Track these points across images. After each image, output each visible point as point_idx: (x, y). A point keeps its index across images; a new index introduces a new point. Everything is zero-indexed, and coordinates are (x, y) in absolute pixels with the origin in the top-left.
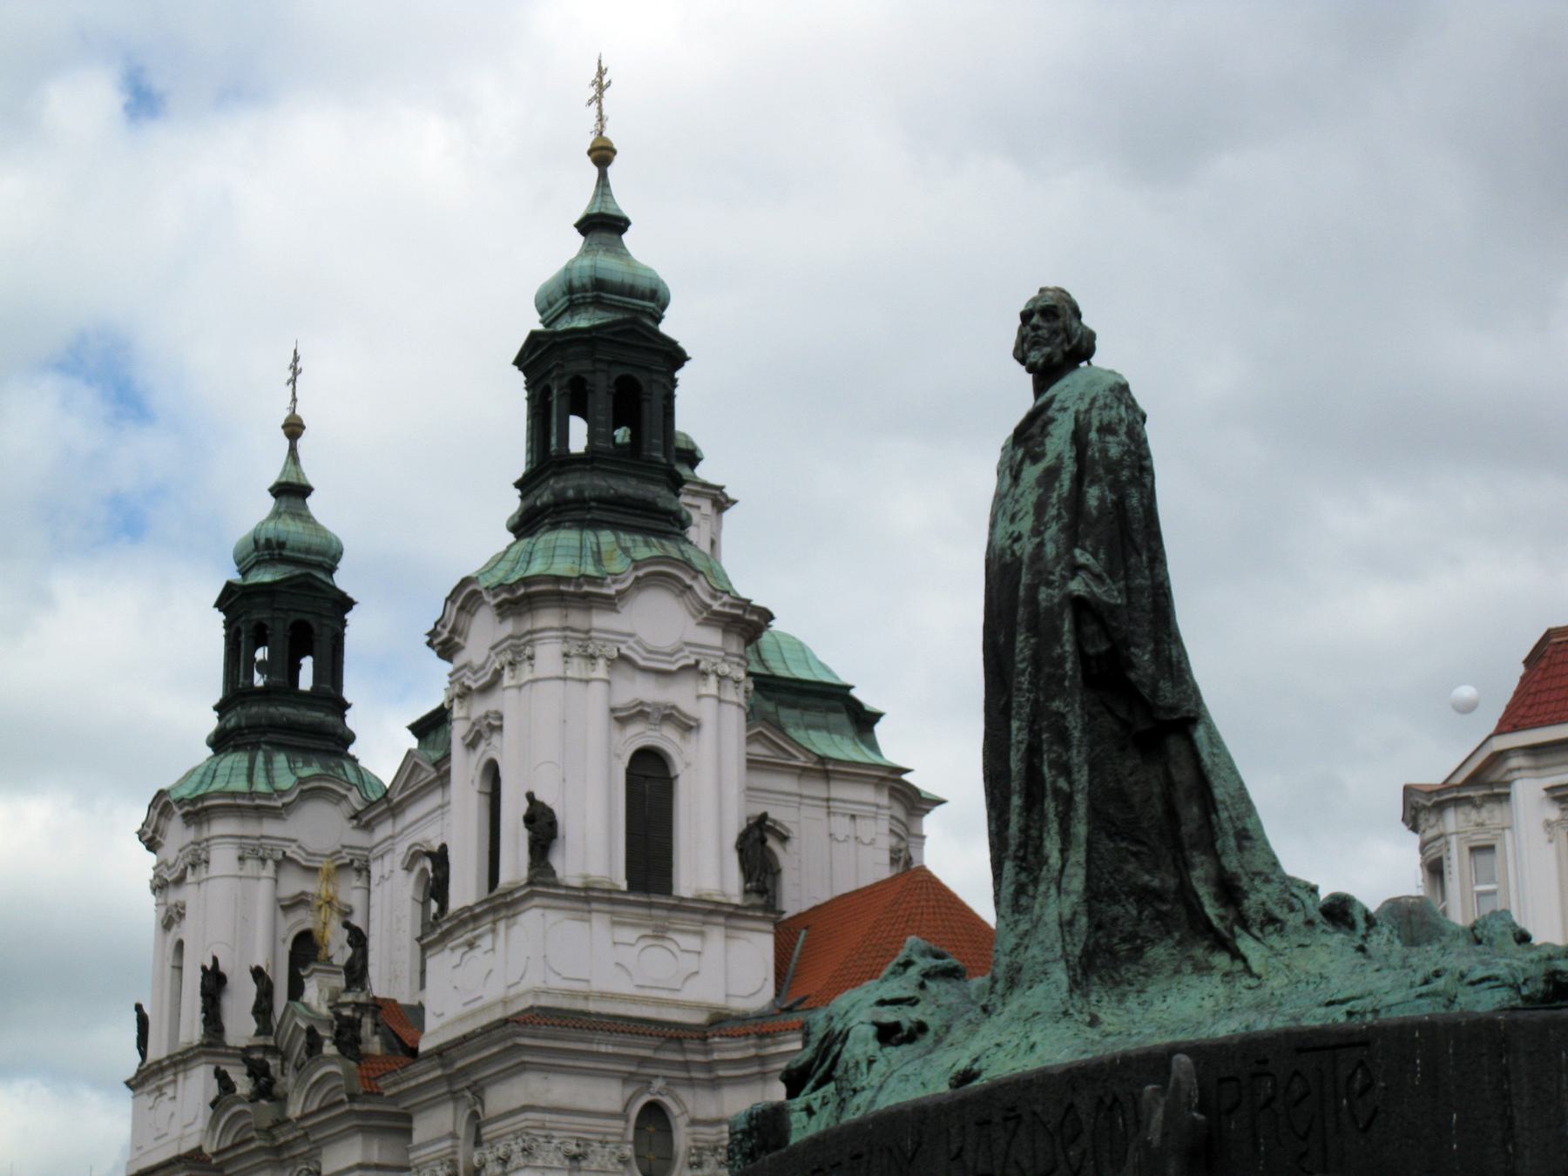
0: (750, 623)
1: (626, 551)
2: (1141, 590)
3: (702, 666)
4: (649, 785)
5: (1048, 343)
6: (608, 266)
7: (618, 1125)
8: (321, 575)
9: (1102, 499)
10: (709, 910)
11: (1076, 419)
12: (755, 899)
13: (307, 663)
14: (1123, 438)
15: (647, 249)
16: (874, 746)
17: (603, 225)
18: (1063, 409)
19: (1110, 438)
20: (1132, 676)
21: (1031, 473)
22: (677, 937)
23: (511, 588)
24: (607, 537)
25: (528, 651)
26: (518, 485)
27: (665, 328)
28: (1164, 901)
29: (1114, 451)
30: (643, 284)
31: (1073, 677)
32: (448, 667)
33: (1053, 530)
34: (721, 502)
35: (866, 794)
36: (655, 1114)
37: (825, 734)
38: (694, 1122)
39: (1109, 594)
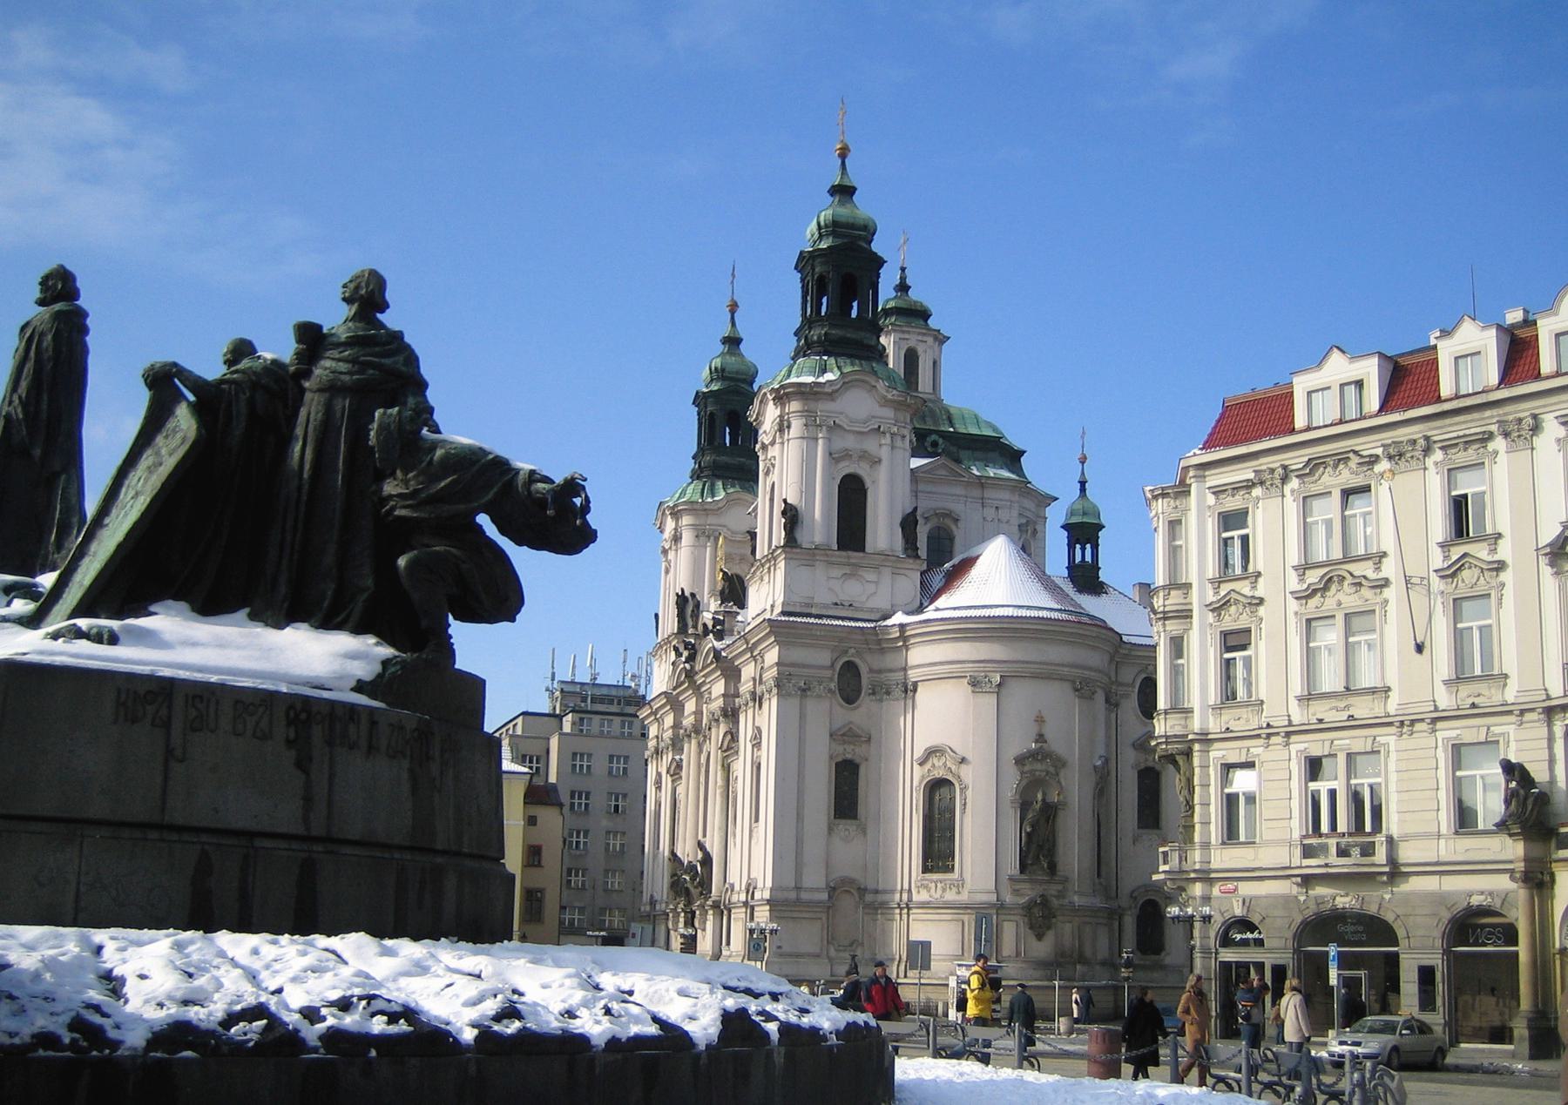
1: (839, 368)
6: (844, 212)
7: (828, 673)
15: (864, 207)
16: (1018, 470)
17: (844, 192)
24: (832, 360)
27: (875, 247)
34: (941, 339)
35: (1005, 495)
38: (871, 671)
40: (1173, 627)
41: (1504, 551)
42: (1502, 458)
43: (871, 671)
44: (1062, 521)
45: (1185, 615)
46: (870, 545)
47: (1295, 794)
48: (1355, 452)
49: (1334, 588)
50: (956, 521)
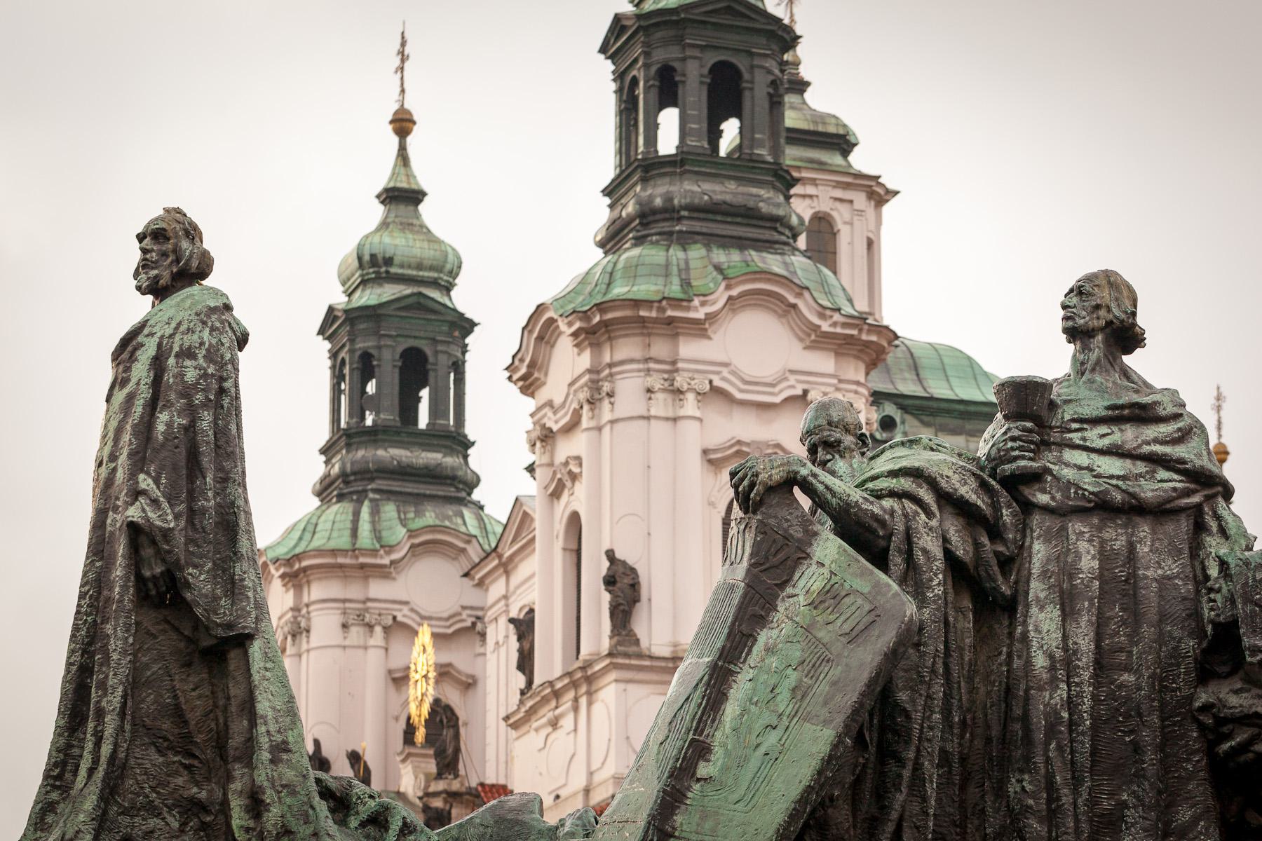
0: (868, 344)
2: (204, 511)
5: (155, 265)
9: (169, 425)
11: (160, 345)
14: (201, 361)
18: (152, 334)
19: (188, 363)
20: (188, 596)
21: (120, 396)
23: (585, 315)
25: (606, 387)
28: (208, 812)
29: (191, 376)
31: (120, 601)
32: (530, 404)
33: (123, 458)
39: (165, 518)
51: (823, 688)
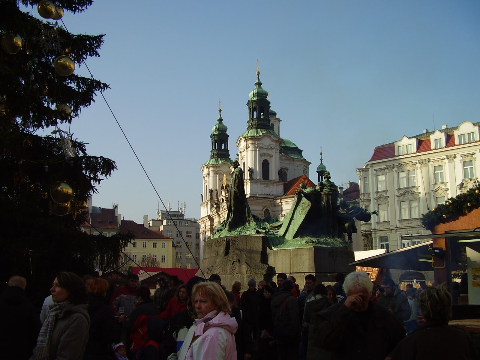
3: (273, 148)
4: (265, 165)
7: (262, 212)
8: (224, 132)
10: (274, 182)
12: (281, 180)
13: (223, 144)
15: (264, 88)
16: (301, 156)
22: (270, 186)
26: (248, 122)
27: (268, 99)
30: (264, 93)
34: (279, 121)
35: (300, 163)
36: (267, 210)
37: (294, 154)
40: (366, 203)
41: (448, 186)
42: (447, 164)
43: (272, 211)
44: (316, 170)
45: (369, 200)
46: (270, 179)
47: (399, 244)
48: (411, 162)
49: (407, 194)
50: (288, 170)
51: (304, 211)
